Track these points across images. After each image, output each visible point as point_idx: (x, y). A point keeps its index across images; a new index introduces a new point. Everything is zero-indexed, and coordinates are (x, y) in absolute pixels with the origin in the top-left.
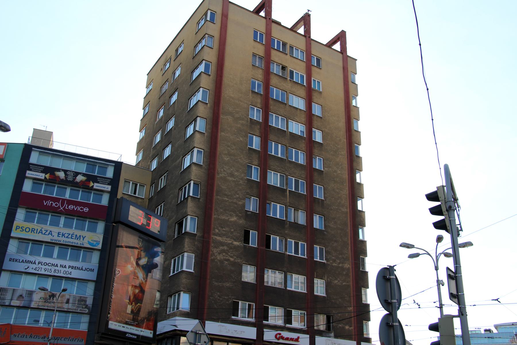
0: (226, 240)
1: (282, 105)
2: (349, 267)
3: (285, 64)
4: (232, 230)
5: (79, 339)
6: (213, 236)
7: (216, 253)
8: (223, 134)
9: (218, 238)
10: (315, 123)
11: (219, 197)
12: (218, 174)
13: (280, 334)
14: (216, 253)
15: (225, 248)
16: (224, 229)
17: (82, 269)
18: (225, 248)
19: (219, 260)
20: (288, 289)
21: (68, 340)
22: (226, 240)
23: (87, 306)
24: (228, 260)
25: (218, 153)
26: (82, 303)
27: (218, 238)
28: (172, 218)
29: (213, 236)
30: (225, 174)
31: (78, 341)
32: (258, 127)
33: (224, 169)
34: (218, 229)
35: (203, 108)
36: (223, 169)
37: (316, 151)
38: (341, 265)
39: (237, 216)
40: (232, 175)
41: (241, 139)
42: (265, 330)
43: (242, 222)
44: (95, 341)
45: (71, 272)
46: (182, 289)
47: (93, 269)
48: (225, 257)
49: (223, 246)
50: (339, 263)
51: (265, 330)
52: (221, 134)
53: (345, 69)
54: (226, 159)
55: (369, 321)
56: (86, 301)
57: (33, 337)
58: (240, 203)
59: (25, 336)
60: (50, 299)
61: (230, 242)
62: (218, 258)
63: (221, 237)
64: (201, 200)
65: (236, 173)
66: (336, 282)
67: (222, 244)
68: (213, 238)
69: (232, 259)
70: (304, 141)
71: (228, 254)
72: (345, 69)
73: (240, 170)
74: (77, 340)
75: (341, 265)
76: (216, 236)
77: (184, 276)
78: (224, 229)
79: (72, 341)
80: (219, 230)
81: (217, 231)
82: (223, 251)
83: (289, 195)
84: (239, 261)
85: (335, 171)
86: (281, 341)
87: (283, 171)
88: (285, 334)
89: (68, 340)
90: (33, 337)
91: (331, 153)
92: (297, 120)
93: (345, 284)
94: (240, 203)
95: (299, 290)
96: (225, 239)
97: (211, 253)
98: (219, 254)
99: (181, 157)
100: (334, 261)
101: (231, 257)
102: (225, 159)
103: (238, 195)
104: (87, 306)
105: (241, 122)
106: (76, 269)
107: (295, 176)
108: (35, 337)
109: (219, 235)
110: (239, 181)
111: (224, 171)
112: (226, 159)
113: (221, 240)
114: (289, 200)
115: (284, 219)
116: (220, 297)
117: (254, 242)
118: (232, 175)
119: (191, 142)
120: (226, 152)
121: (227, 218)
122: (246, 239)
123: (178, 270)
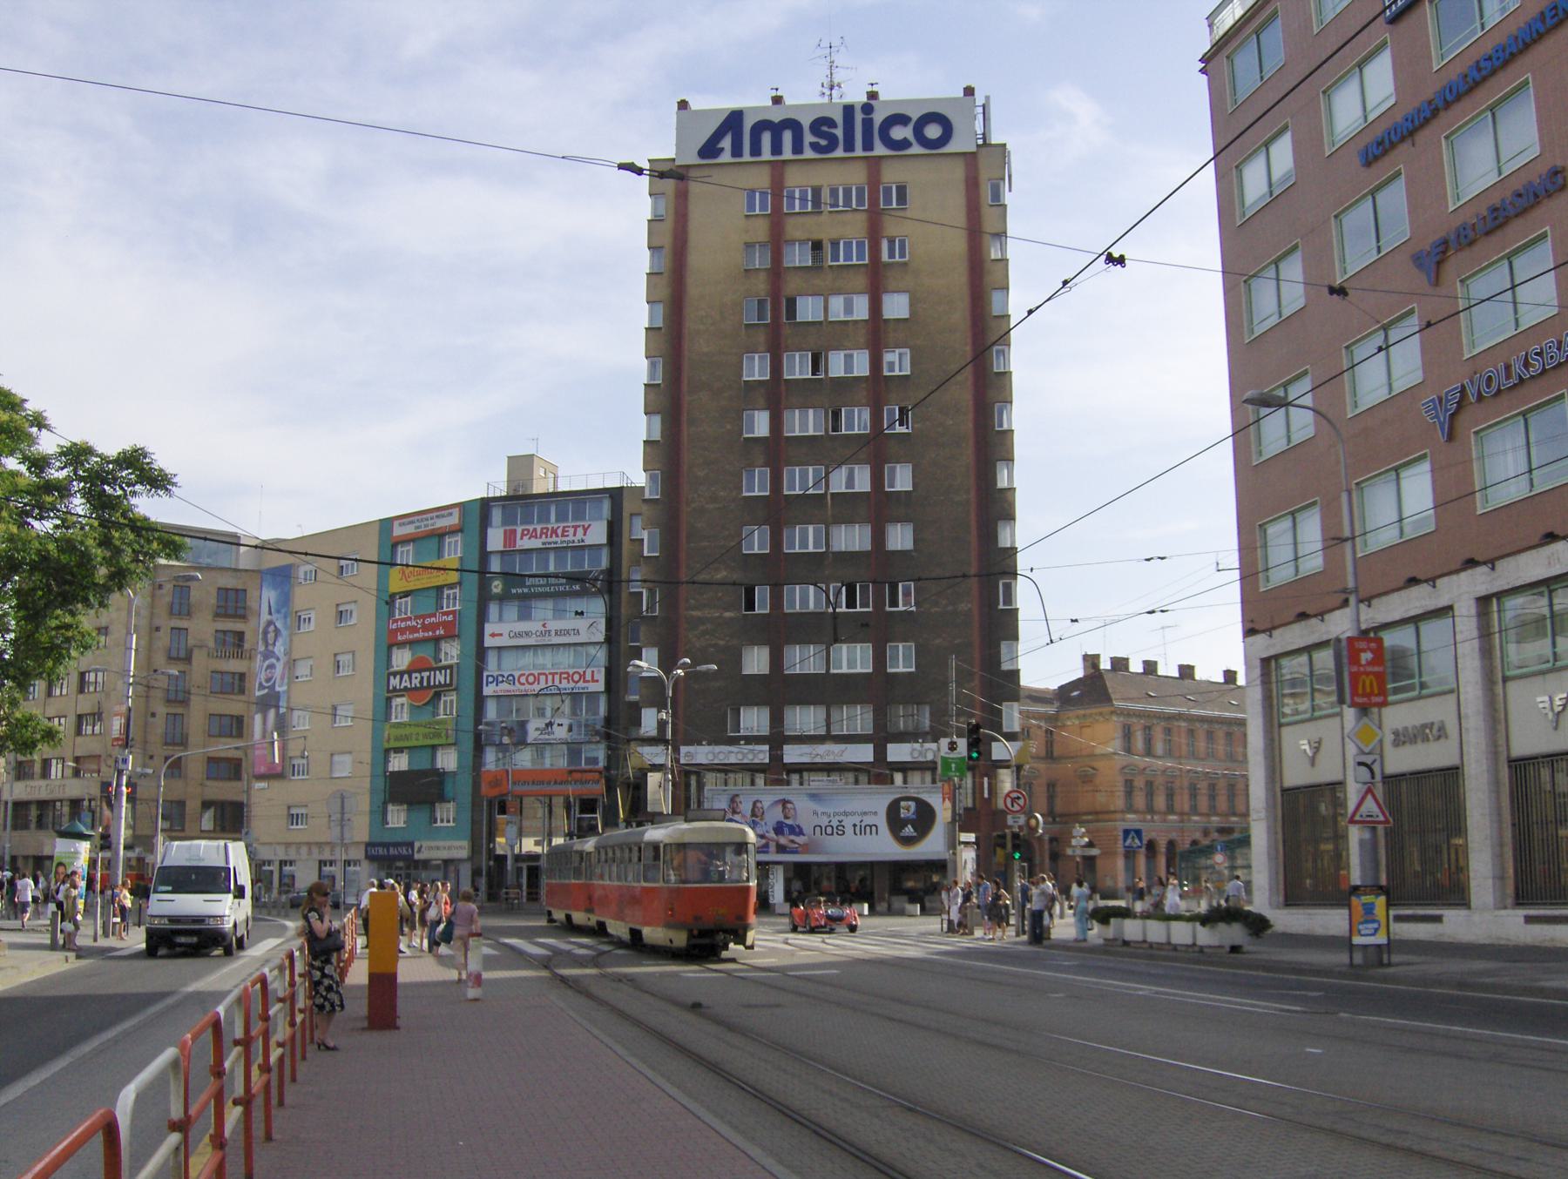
9: (694, 613)
20: (833, 671)
24: (715, 645)
27: (694, 613)
67: (701, 621)
81: (692, 601)
95: (859, 670)
117: (762, 608)
122: (750, 605)
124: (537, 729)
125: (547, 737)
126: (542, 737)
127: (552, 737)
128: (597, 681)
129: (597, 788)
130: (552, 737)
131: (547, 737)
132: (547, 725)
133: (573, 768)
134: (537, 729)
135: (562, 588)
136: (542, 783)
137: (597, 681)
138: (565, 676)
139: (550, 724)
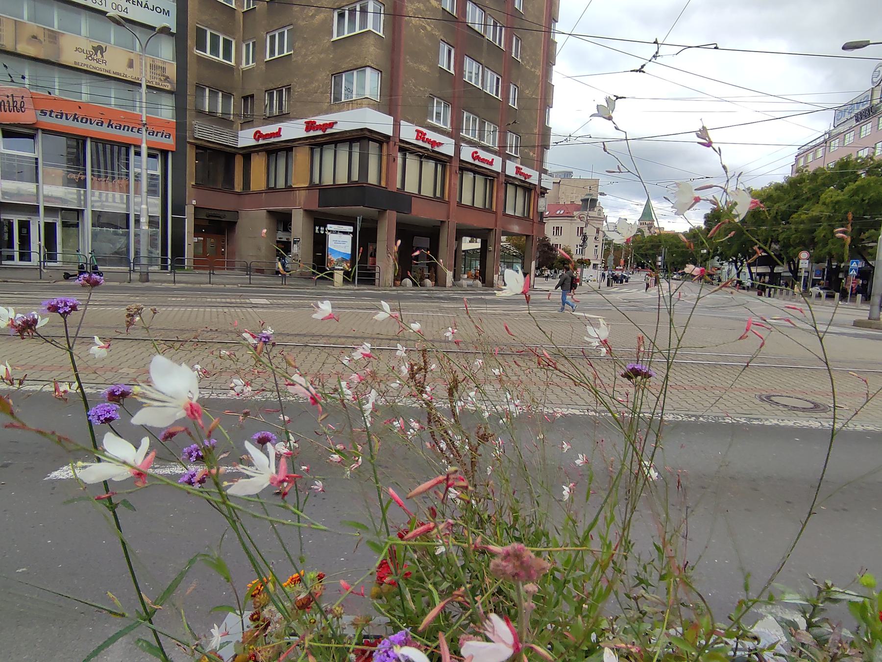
5: (163, 133)
13: (476, 152)
17: (146, 6)
19: (414, 25)
23: (168, 77)
26: (159, 72)
31: (162, 137)
44: (188, 140)
45: (127, 8)
46: (369, 63)
47: (168, 11)
48: (421, 23)
50: (532, 67)
55: (547, 149)
56: (164, 69)
57: (79, 120)
59: (64, 117)
60: (96, 54)
62: (414, 22)
74: (160, 135)
75: (533, 70)
77: (371, 40)
86: (477, 162)
88: (483, 154)
90: (79, 120)
104: (167, 79)
106: (136, 3)
108: (84, 121)
116: (415, 87)
123: (344, 34)
125: (94, 63)
126: (88, 62)
129: (169, 143)
130: (103, 66)
131: (94, 63)
136: (87, 120)
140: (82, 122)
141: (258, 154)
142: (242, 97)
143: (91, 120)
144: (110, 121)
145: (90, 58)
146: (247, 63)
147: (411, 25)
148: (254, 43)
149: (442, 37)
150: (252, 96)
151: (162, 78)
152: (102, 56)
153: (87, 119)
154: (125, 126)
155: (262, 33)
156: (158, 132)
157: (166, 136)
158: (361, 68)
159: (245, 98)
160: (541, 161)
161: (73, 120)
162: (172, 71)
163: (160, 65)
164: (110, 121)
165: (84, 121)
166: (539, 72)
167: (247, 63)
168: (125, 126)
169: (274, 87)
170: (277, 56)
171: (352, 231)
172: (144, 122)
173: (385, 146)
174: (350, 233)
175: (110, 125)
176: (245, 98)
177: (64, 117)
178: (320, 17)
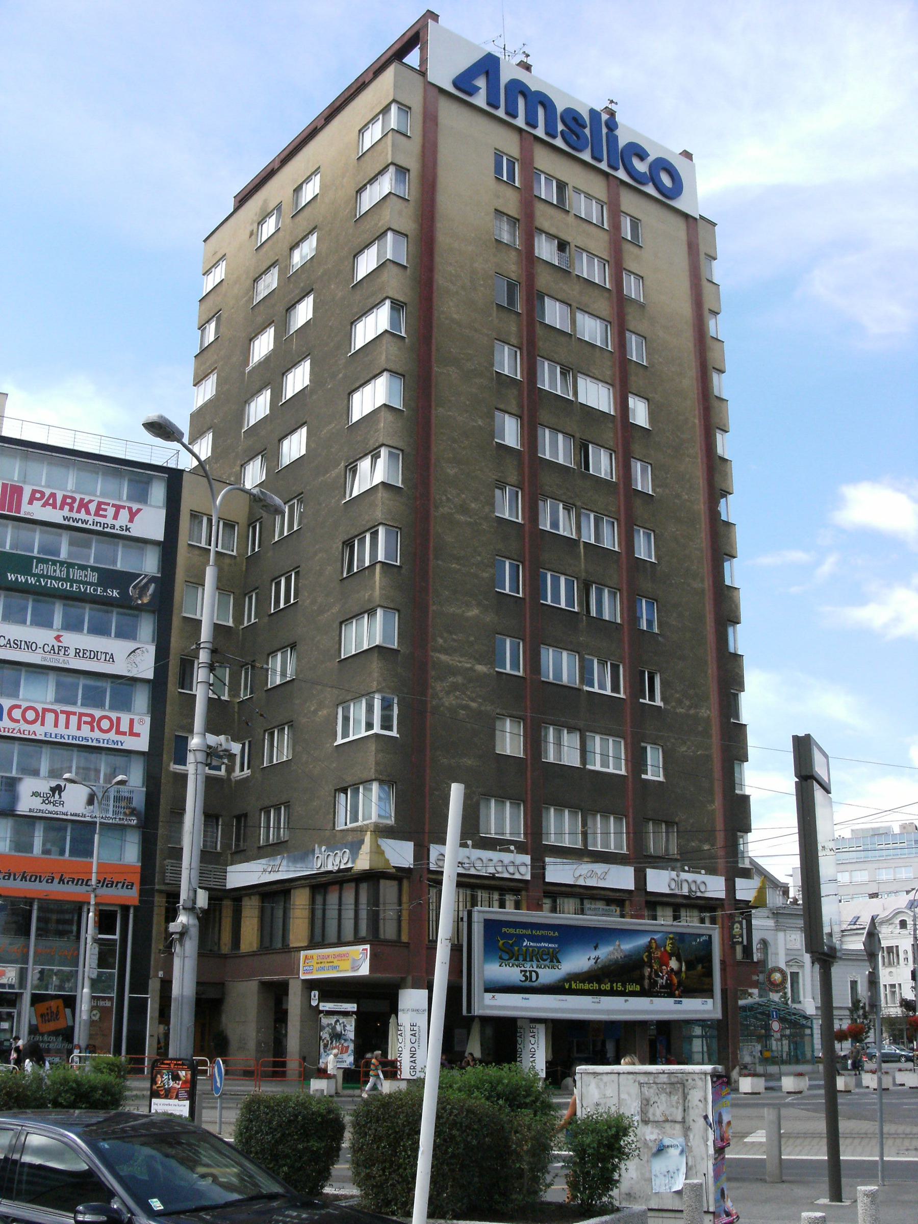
0: (460, 662)
1: (563, 339)
2: (709, 717)
3: (564, 236)
4: (472, 639)
5: (124, 883)
6: (432, 654)
7: (441, 691)
8: (440, 410)
9: (443, 657)
10: (635, 381)
11: (440, 562)
12: (437, 507)
14: (441, 691)
15: (459, 679)
16: (454, 637)
18: (459, 679)
20: (589, 767)
21: (102, 886)
22: (460, 662)
25: (433, 457)
26: (123, 804)
27: (443, 657)
28: (328, 610)
29: (432, 654)
30: (450, 508)
32: (515, 392)
33: (449, 496)
34: (442, 637)
35: (396, 349)
36: (446, 496)
37: (637, 448)
38: (692, 712)
39: (479, 604)
40: (464, 509)
41: (480, 423)
42: (547, 859)
43: (489, 618)
48: (459, 701)
49: (454, 675)
50: (690, 707)
51: (547, 859)
52: (439, 412)
53: (693, 248)
54: (451, 471)
56: (130, 800)
57: (28, 878)
58: (485, 575)
59: (12, 877)
60: (54, 795)
61: (469, 665)
62: (447, 704)
63: (447, 654)
64: (403, 571)
65: (473, 505)
66: (684, 749)
67: (453, 671)
68: (432, 657)
69: (474, 705)
70: (611, 425)
71: (465, 694)
72: (693, 248)
73: (482, 498)
74: (120, 885)
75: (692, 712)
76: (439, 652)
78: (454, 637)
79: (112, 886)
80: (445, 641)
81: (440, 641)
82: (455, 687)
83: (584, 552)
84: (489, 708)
85: (678, 496)
87: (571, 498)
89: (102, 886)
90: (28, 878)
91: (669, 451)
92: (594, 373)
93: (701, 754)
94: (485, 575)
96: (457, 659)
97: (430, 691)
98: (448, 693)
99: (343, 464)
100: (680, 702)
101: (473, 700)
102: (449, 471)
103: (480, 555)
105: (477, 381)
107: (595, 510)
108: (33, 879)
109: (446, 651)
110: (481, 524)
111: (448, 499)
112: (451, 471)
113: (451, 662)
114: (585, 566)
115: (576, 610)
118: (464, 509)
119: (372, 433)
120: (451, 455)
121: (459, 611)
124: (36, 794)
125: (50, 807)
126: (44, 807)
127: (60, 809)
128: (138, 735)
130: (60, 809)
131: (50, 807)
132: (53, 790)
133: (721, 863)
134: (36, 794)
135: (90, 590)
136: (38, 878)
137: (138, 735)
138: (88, 719)
139: (58, 789)
140: (30, 880)
141: (250, 898)
142: (234, 817)
143: (40, 876)
144: (62, 875)
145: (47, 802)
146: (242, 770)
147: (442, 709)
148: (250, 742)
149: (498, 711)
150: (246, 815)
151: (127, 811)
152: (60, 797)
153: (36, 877)
154: (78, 880)
155: (259, 730)
156: (117, 883)
157: (127, 886)
158: (367, 782)
159: (238, 818)
160: (733, 849)
161: (21, 880)
162: (139, 801)
163: (126, 794)
164: (62, 875)
165: (33, 879)
166: (710, 711)
167: (242, 770)
168: (78, 880)
169: (271, 804)
170: (275, 762)
171: (355, 1010)
172: (94, 887)
173: (405, 883)
174: (353, 1013)
175: (61, 880)
176: (238, 818)
177: (12, 877)
178: (323, 713)
